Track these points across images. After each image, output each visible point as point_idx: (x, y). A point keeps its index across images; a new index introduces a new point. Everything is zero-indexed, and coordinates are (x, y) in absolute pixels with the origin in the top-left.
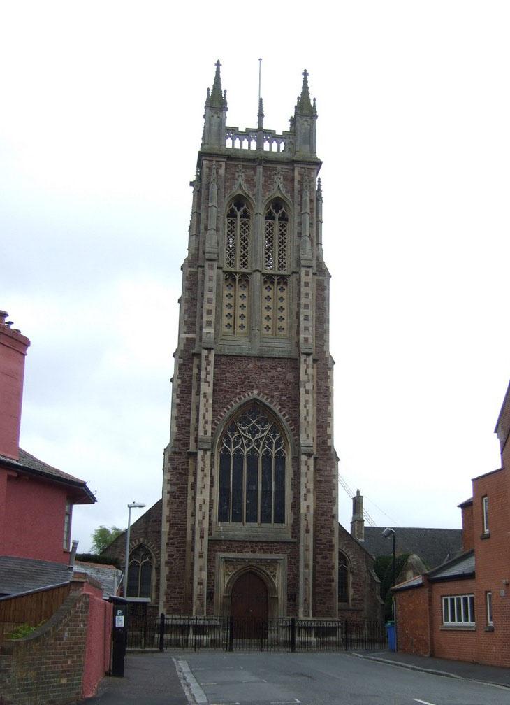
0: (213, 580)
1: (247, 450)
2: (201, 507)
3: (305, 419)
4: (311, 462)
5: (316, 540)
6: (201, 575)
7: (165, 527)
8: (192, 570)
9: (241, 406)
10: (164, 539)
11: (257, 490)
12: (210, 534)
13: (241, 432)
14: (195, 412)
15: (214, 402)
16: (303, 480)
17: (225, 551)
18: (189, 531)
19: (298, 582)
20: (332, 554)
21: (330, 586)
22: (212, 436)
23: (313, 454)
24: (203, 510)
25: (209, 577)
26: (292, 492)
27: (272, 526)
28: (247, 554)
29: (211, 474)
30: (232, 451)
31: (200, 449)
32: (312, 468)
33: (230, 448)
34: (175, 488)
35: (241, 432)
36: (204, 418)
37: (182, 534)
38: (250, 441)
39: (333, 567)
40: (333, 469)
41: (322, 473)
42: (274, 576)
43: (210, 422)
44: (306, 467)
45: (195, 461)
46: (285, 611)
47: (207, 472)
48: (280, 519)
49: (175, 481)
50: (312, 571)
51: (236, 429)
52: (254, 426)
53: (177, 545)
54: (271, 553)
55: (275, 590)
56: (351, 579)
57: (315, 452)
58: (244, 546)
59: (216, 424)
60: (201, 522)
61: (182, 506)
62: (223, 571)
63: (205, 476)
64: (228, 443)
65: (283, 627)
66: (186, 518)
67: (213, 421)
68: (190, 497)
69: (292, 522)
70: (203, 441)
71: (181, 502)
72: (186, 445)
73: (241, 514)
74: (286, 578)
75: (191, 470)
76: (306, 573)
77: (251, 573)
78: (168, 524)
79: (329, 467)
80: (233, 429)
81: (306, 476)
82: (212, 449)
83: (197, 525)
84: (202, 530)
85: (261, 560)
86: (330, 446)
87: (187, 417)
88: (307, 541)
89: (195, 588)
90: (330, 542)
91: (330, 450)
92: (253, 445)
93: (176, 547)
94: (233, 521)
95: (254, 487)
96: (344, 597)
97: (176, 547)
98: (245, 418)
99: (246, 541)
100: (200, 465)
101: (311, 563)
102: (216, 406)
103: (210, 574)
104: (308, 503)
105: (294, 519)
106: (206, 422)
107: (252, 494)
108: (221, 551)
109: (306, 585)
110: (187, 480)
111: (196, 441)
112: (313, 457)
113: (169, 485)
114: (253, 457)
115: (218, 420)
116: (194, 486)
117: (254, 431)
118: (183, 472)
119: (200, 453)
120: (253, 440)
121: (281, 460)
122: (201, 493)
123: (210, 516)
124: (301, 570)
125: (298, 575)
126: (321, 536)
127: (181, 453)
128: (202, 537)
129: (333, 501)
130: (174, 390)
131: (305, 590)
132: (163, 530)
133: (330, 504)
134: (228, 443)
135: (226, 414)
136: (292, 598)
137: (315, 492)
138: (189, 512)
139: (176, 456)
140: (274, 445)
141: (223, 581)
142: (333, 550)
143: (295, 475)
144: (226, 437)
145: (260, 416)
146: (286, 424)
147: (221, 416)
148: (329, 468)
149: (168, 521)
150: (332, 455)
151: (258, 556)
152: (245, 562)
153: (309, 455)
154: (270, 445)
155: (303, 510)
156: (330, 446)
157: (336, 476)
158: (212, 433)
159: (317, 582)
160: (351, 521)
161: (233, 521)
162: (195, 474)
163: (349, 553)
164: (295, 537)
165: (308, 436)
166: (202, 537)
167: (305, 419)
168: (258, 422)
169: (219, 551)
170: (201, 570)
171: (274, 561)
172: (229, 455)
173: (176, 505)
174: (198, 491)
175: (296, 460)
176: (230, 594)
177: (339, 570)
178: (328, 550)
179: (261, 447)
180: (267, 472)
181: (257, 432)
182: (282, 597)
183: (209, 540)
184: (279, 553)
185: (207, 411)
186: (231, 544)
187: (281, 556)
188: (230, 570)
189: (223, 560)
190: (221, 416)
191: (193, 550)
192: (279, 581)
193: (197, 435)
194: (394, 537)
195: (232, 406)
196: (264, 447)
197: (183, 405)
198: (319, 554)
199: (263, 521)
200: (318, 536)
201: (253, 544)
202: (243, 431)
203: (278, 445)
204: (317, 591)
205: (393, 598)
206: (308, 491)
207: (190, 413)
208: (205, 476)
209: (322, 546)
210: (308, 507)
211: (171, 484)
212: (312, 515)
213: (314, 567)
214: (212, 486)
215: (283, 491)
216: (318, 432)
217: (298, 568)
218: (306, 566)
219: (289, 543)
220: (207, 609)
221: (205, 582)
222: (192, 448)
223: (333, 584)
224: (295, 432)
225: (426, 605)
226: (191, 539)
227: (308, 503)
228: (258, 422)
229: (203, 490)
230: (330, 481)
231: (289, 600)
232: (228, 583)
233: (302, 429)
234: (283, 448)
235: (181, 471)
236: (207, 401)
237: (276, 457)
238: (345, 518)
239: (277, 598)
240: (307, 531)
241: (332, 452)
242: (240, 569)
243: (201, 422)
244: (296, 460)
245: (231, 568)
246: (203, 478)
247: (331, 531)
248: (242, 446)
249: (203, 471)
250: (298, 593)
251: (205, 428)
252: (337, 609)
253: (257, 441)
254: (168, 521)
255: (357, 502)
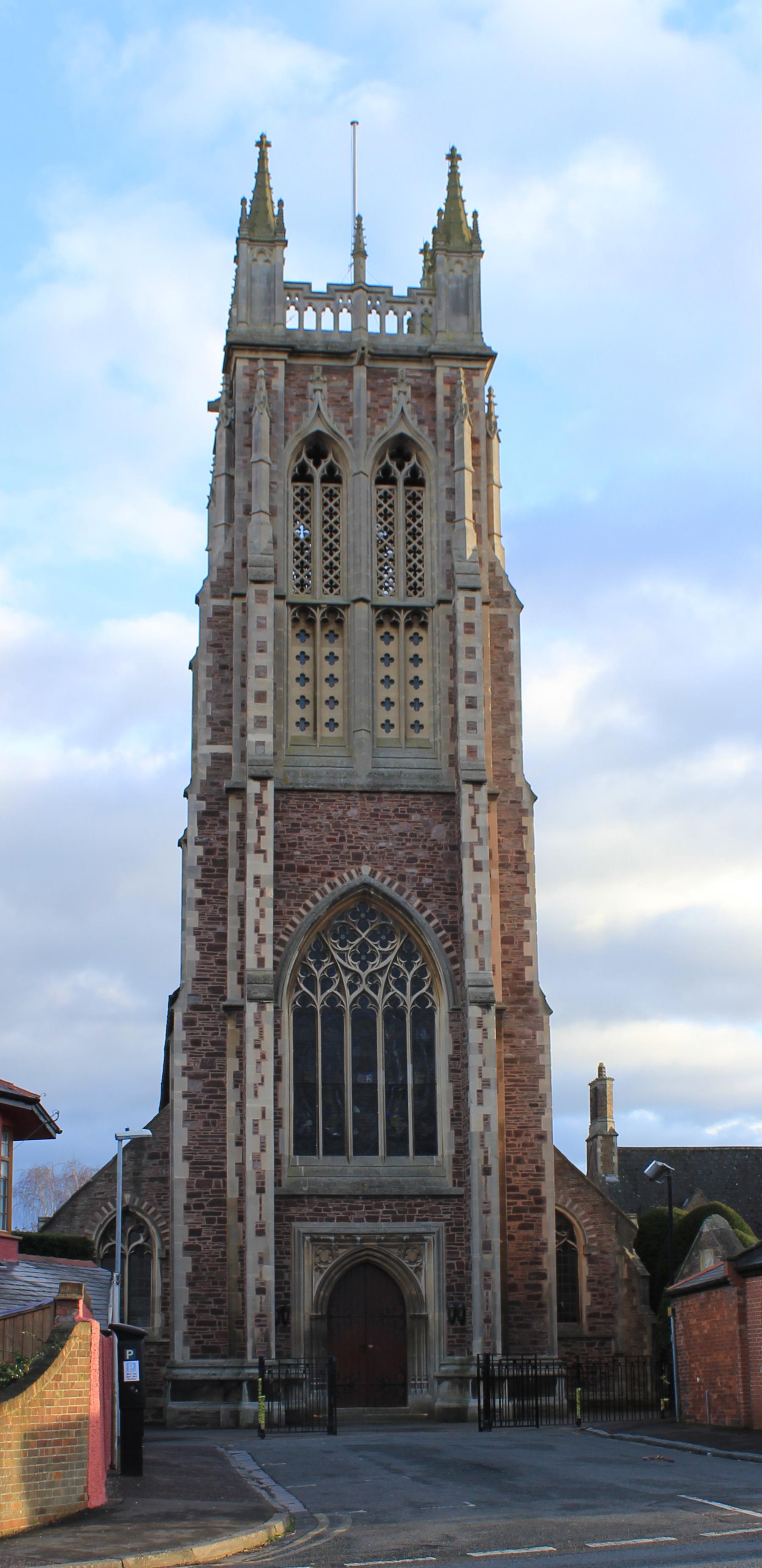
0: (288, 1283)
1: (350, 998)
2: (256, 1125)
3: (475, 926)
4: (490, 1018)
5: (508, 1189)
6: (261, 1272)
7: (180, 1171)
8: (242, 1261)
9: (335, 902)
10: (180, 1197)
11: (374, 1085)
12: (278, 1183)
13: (337, 957)
14: (237, 918)
15: (278, 894)
16: (474, 1060)
17: (312, 1220)
18: (232, 1178)
19: (469, 1280)
20: (540, 1219)
21: (539, 1287)
22: (275, 969)
23: (494, 1002)
24: (261, 1132)
25: (278, 1275)
26: (451, 1086)
27: (411, 1160)
28: (358, 1225)
29: (276, 1053)
30: (319, 1000)
31: (251, 1000)
32: (492, 1033)
33: (315, 993)
34: (199, 1085)
35: (337, 957)
36: (257, 930)
37: (218, 1185)
38: (356, 976)
39: (543, 1248)
40: (538, 1033)
41: (515, 1041)
42: (418, 1270)
43: (269, 939)
44: (480, 1030)
45: (240, 1024)
46: (444, 1341)
47: (264, 1047)
48: (427, 1145)
49: (197, 1069)
50: (498, 1257)
51: (326, 953)
52: (364, 945)
53: (207, 1209)
54: (410, 1219)
55: (420, 1300)
56: (584, 1269)
57: (499, 998)
58: (350, 1208)
59: (282, 943)
60: (257, 1159)
61: (214, 1124)
62: (308, 1260)
63: (263, 1057)
64: (310, 982)
65: (440, 1379)
66: (224, 1150)
67: (276, 935)
68: (231, 1105)
69: (453, 1152)
70: (254, 981)
71: (212, 1116)
72: (219, 991)
73: (342, 1138)
74: (443, 1274)
75: (231, 1046)
76: (486, 1264)
77: (367, 1264)
78: (186, 1165)
79: (530, 1028)
80: (320, 952)
81: (481, 1052)
82: (275, 997)
83: (249, 1166)
84: (260, 1176)
85: (389, 1236)
86: (531, 984)
87: (220, 929)
88: (486, 1192)
89: (249, 1303)
90: (536, 1192)
91: (530, 990)
92: (363, 986)
93: (205, 1214)
94: (326, 1153)
95: (368, 1079)
96: (569, 1311)
97: (205, 1214)
98: (344, 927)
99: (356, 1197)
100: (252, 1033)
101: (496, 1241)
102: (281, 902)
103: (281, 1271)
104: (487, 1110)
105: (458, 1145)
106: (262, 940)
107: (365, 1094)
108: (302, 1219)
109: (487, 1287)
110: (223, 1067)
111: (241, 981)
112: (493, 1009)
113: (186, 1079)
114: (364, 1018)
115: (287, 933)
116: (239, 1079)
117: (364, 955)
118: (214, 1049)
119: (251, 1008)
120: (364, 975)
121: (424, 1016)
122: (256, 1095)
123: (276, 1144)
124: (476, 1254)
125: (469, 1267)
126: (517, 1181)
127: (208, 1008)
128: (261, 1190)
129: (539, 1105)
130: (186, 870)
131: (486, 1300)
132: (176, 1177)
133: (535, 1109)
134: (310, 982)
135: (302, 917)
136: (458, 1315)
137: (502, 1085)
138: (231, 1136)
139: (198, 1015)
140: (409, 984)
141: (309, 1285)
142: (542, 1210)
143: (456, 1048)
144: (306, 969)
145: (377, 922)
146: (432, 940)
147: (293, 924)
148: (529, 1032)
149: (186, 1158)
150: (535, 1000)
151: (383, 1227)
152: (356, 1241)
153: (486, 1005)
154: (401, 984)
155: (476, 1125)
156: (531, 984)
157: (544, 1049)
158: (275, 963)
159: (512, 1280)
160: (587, 1135)
161: (326, 1153)
162: (240, 1054)
163: (579, 1217)
164: (461, 1184)
165: (482, 963)
166: (261, 1190)
167: (475, 926)
168: (373, 936)
169: (299, 1220)
170: (261, 1261)
171: (418, 1238)
172: (314, 1010)
173: (201, 1121)
174: (249, 1091)
175: (457, 1013)
176: (324, 1313)
177: (558, 1252)
178: (534, 1210)
179: (381, 990)
180: (395, 1043)
181: (372, 957)
182: (435, 1314)
183: (276, 1196)
184: (426, 1220)
185: (262, 915)
186: (322, 1202)
187: (434, 1226)
188: (324, 1259)
189: (308, 1238)
190: (293, 924)
191: (241, 1218)
192: (429, 1280)
193: (243, 967)
194: (669, 1179)
195: (315, 901)
196: (387, 989)
197: (209, 902)
198: (511, 1218)
199: (390, 1152)
200: (509, 1180)
201: (372, 1199)
202: (342, 955)
203: (417, 984)
204: (511, 1299)
205: (669, 1309)
206: (486, 1083)
207: (225, 919)
208: (263, 1057)
209: (520, 1203)
210: (486, 1118)
211: (191, 1077)
212: (496, 1137)
213: (503, 1247)
214: (278, 1078)
215: (432, 1085)
216: (505, 952)
217: (468, 1250)
218: (487, 1246)
219: (449, 1197)
220: (277, 1346)
221: (271, 1288)
222: (233, 992)
223: (545, 1284)
224: (453, 954)
225: (735, 1323)
226: (237, 1195)
227: (487, 1110)
228: (373, 936)
229: (260, 1088)
230: (532, 1060)
231: (451, 1321)
232: (320, 1288)
233: (469, 948)
234: (430, 990)
235: (210, 1047)
236: (262, 893)
237: (414, 1010)
238: (569, 1132)
239: (426, 1318)
240: (487, 1171)
241: (536, 994)
242: (345, 1258)
243: (251, 939)
244: (457, 1013)
245: (325, 1255)
246: (258, 1063)
247: (539, 1169)
248: (340, 988)
249: (257, 1046)
250: (470, 1305)
251: (258, 953)
252: (556, 1336)
253: (371, 976)
254: (186, 1158)
255: (599, 1097)
